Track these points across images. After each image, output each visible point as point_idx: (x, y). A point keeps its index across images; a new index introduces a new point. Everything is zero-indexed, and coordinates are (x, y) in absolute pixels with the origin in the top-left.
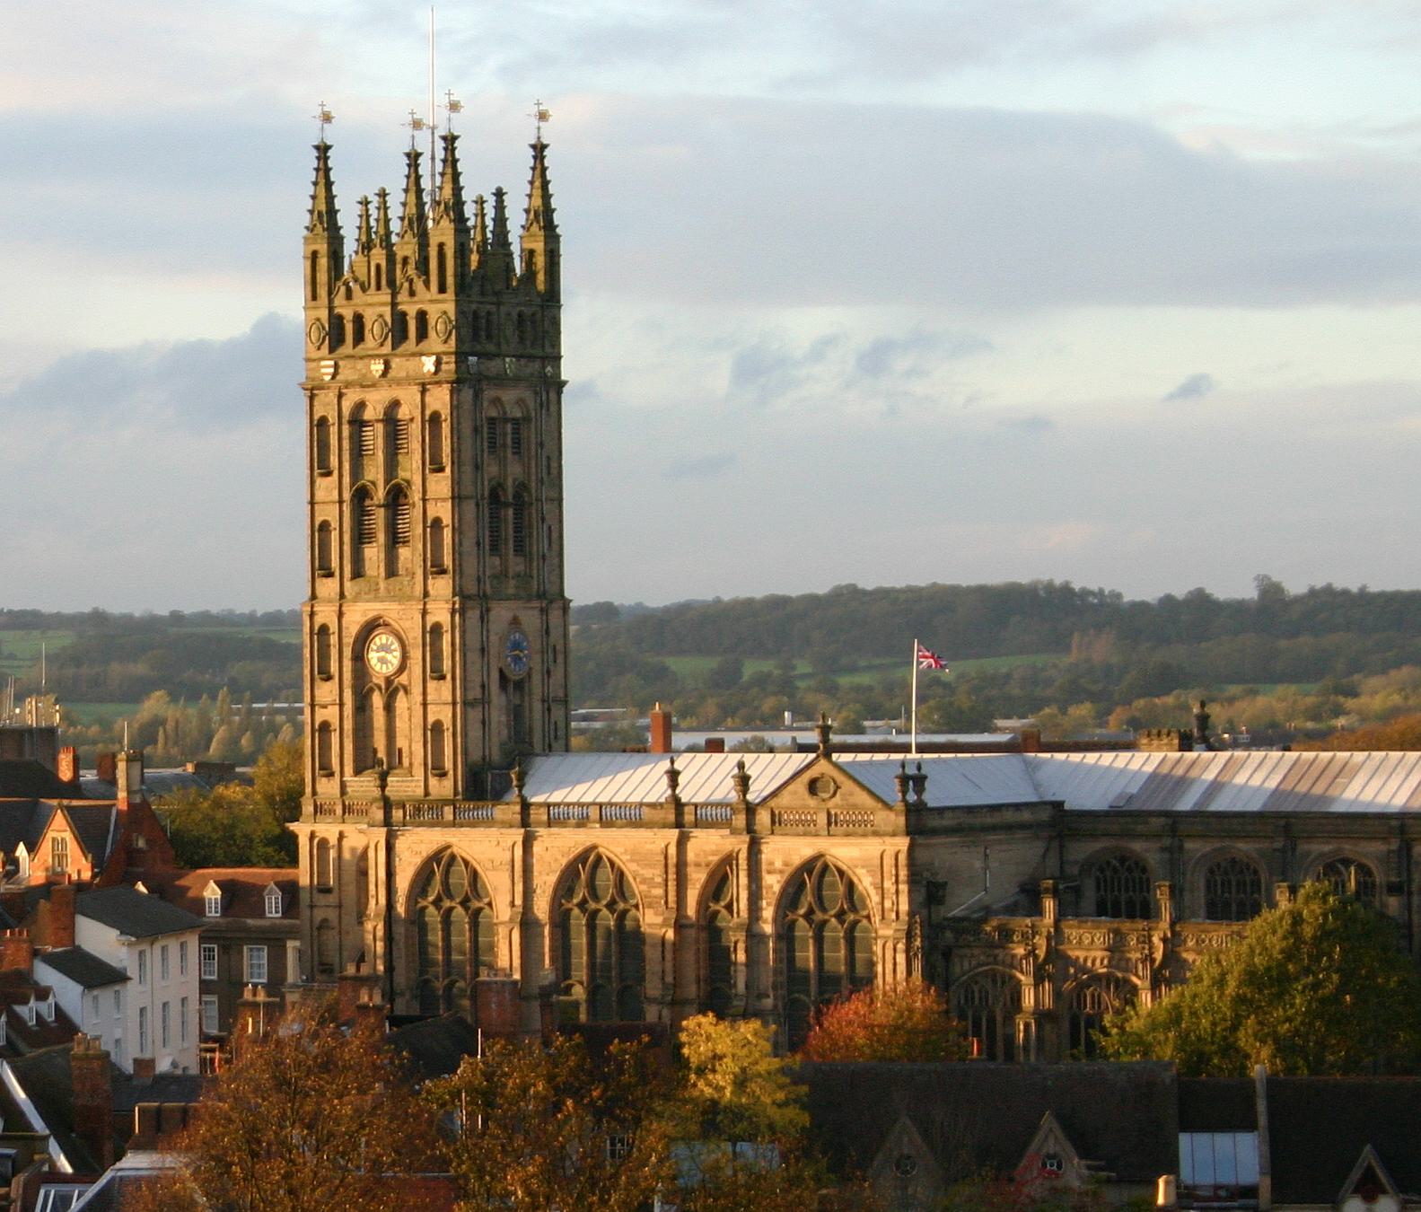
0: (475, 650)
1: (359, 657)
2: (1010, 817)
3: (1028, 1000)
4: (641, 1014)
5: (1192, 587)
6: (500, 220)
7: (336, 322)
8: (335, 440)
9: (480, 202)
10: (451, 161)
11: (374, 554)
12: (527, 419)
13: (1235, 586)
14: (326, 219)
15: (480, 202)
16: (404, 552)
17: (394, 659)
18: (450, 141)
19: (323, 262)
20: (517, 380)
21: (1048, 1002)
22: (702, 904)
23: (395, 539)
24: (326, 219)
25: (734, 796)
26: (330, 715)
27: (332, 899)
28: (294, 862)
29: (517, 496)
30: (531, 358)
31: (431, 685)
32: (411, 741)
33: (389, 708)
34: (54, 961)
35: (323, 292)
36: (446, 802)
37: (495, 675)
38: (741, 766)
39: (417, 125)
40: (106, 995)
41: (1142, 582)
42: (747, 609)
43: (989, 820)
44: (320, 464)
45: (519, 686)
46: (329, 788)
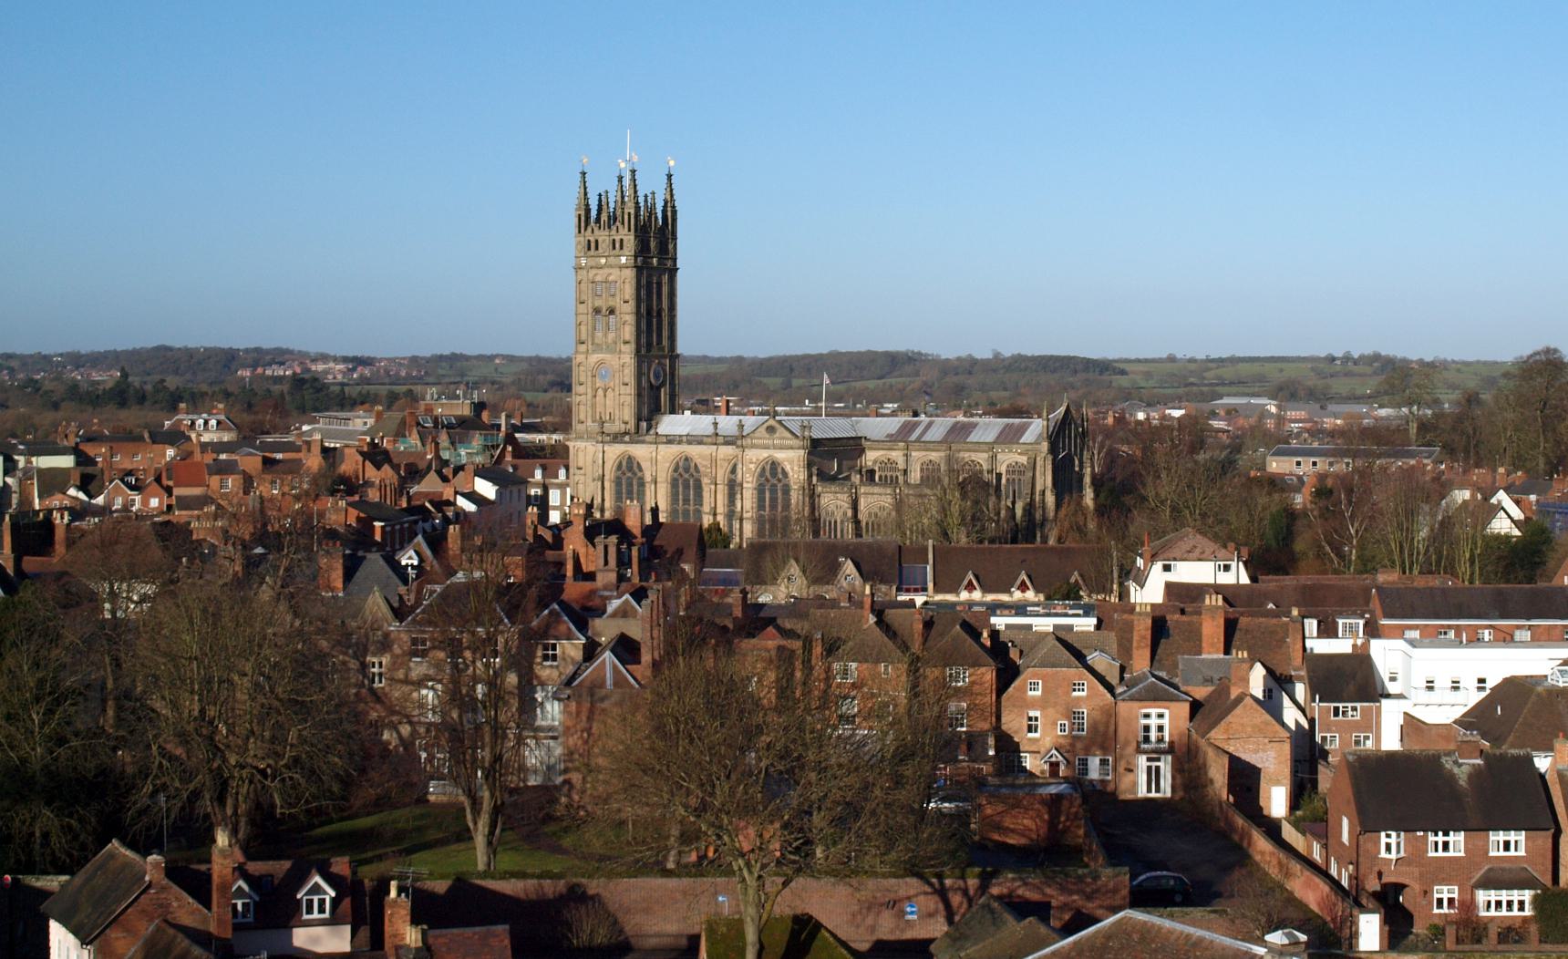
0: (639, 375)
5: (1539, 347)
13: (983, 353)
18: (633, 172)
41: (948, 350)
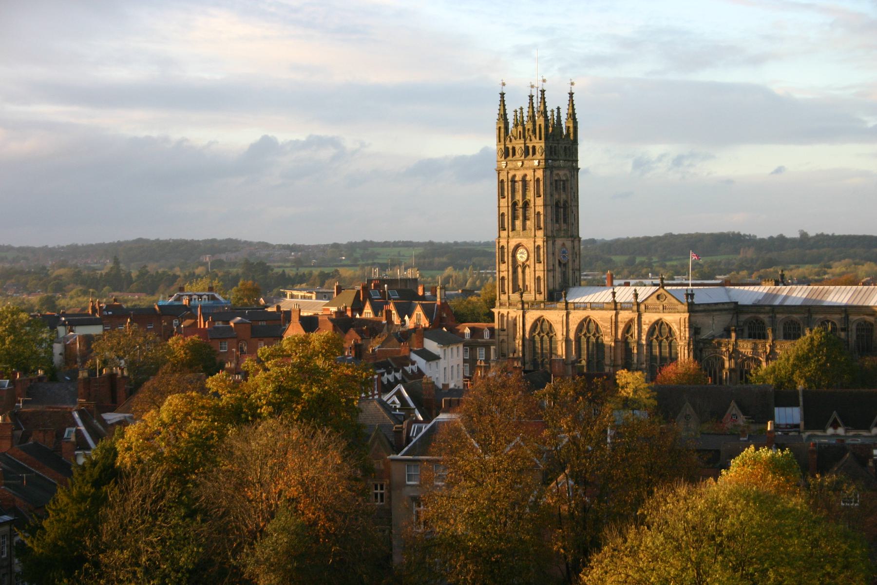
1: (514, 256)
2: (721, 307)
3: (727, 365)
4: (603, 369)
6: (559, 117)
7: (507, 149)
8: (507, 187)
9: (552, 111)
10: (543, 98)
11: (519, 223)
12: (567, 180)
13: (793, 233)
14: (503, 116)
15: (552, 111)
16: (528, 223)
17: (525, 256)
18: (543, 92)
19: (502, 130)
20: (564, 168)
21: (733, 366)
22: (623, 334)
23: (525, 218)
24: (503, 116)
25: (633, 300)
26: (505, 274)
27: (505, 333)
28: (493, 321)
29: (564, 205)
30: (569, 161)
31: (537, 265)
32: (530, 283)
33: (523, 272)
34: (416, 352)
35: (502, 140)
36: (541, 302)
37: (557, 262)
38: (635, 290)
39: (532, 86)
40: (433, 364)
41: (763, 232)
42: (637, 240)
43: (714, 308)
44: (502, 195)
45: (565, 265)
46: (504, 298)
